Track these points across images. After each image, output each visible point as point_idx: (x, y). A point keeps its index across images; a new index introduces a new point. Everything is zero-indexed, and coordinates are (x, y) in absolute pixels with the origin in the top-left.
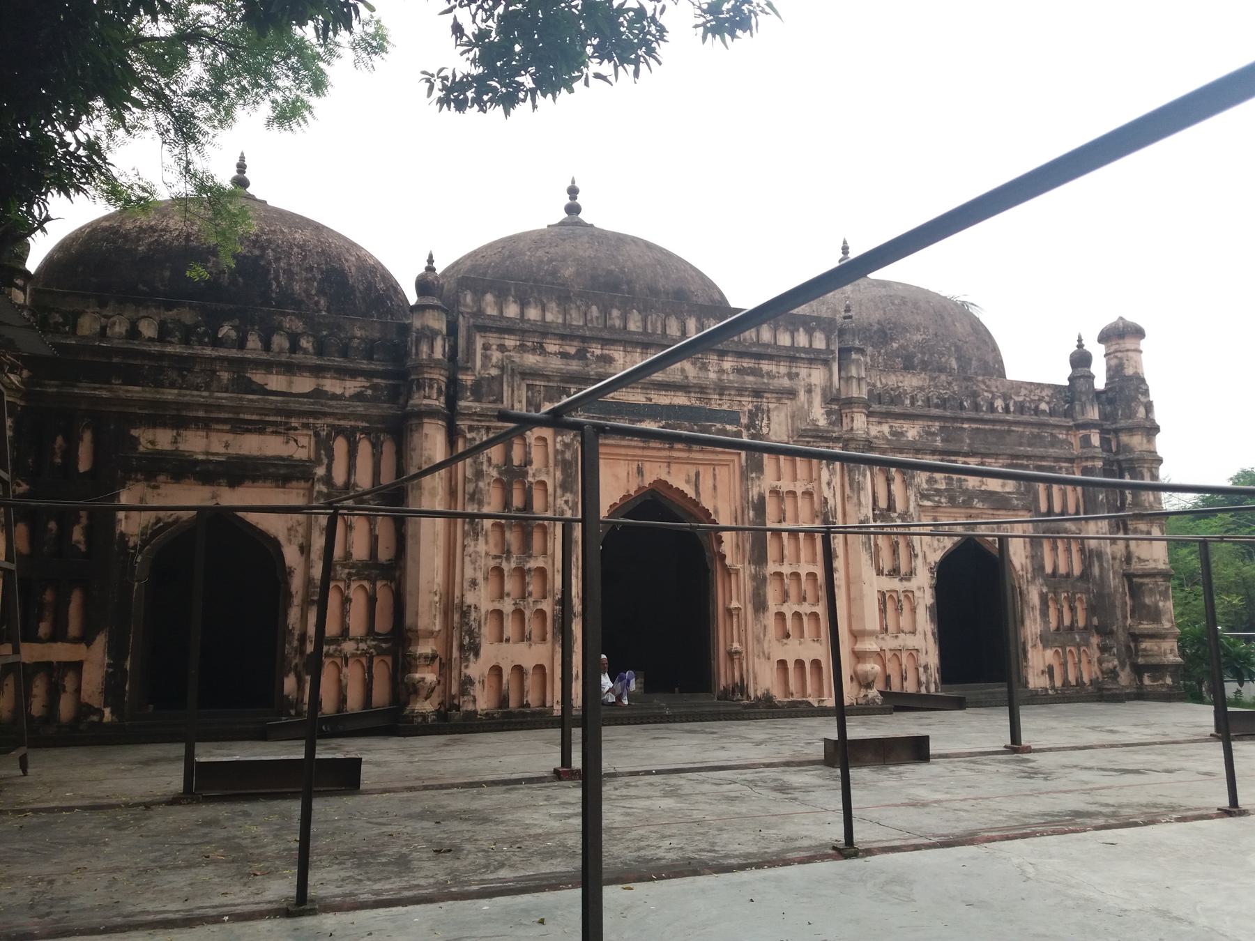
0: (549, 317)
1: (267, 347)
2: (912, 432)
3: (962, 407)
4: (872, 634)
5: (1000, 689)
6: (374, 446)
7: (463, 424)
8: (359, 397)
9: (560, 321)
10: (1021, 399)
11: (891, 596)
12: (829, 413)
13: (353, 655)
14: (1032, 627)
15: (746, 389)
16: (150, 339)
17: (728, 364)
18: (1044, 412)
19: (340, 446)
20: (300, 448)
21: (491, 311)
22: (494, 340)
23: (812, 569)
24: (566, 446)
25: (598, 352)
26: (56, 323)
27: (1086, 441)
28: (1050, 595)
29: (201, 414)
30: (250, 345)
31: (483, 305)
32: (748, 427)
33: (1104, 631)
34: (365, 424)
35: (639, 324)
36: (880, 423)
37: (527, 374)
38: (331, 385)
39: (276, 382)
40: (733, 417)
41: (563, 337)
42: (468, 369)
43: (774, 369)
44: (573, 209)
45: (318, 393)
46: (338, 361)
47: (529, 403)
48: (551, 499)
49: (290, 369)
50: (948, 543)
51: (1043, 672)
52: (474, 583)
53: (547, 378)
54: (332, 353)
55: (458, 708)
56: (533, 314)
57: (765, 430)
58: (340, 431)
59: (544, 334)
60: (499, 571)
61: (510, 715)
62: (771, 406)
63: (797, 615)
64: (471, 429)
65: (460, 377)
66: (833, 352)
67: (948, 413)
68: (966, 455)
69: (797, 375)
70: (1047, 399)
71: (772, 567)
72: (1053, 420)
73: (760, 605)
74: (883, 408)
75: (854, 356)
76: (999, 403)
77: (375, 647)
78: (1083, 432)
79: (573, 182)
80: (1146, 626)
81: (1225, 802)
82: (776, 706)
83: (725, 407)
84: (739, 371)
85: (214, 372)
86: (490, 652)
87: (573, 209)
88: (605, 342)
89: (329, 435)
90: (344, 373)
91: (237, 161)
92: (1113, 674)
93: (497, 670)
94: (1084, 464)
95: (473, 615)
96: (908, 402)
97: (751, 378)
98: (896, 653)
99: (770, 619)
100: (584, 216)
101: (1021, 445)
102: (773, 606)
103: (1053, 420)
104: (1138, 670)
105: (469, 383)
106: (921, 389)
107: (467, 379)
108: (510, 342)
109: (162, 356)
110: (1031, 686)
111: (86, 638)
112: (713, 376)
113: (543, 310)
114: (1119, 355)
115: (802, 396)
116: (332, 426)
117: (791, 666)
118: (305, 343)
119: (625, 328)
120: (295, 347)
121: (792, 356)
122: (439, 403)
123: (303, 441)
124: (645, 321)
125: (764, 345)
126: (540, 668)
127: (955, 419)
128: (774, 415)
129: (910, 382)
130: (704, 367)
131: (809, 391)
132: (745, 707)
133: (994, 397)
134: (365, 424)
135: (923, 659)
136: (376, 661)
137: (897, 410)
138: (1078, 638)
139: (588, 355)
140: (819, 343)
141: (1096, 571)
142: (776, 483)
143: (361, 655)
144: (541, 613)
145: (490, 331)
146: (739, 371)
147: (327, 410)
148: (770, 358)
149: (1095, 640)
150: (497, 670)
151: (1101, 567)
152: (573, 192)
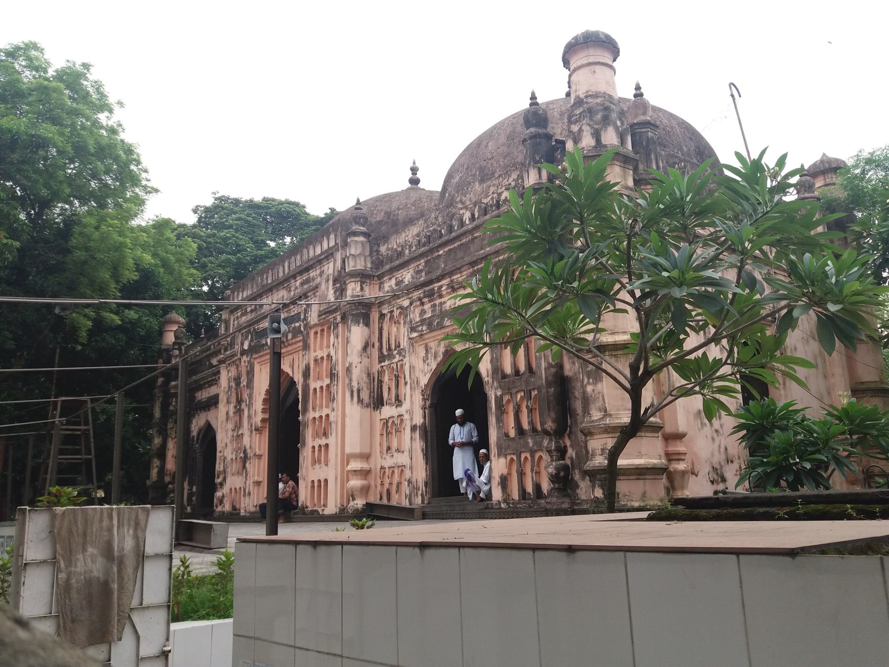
2: (407, 275)
3: (441, 236)
11: (393, 422)
12: (335, 292)
28: (506, 398)
36: (390, 279)
43: (314, 274)
44: (414, 181)
50: (434, 366)
63: (320, 446)
68: (439, 279)
70: (513, 184)
79: (414, 163)
84: (302, 284)
87: (414, 181)
96: (407, 252)
112: (292, 293)
117: (316, 484)
131: (328, 281)
138: (530, 442)
142: (315, 354)
152: (414, 170)
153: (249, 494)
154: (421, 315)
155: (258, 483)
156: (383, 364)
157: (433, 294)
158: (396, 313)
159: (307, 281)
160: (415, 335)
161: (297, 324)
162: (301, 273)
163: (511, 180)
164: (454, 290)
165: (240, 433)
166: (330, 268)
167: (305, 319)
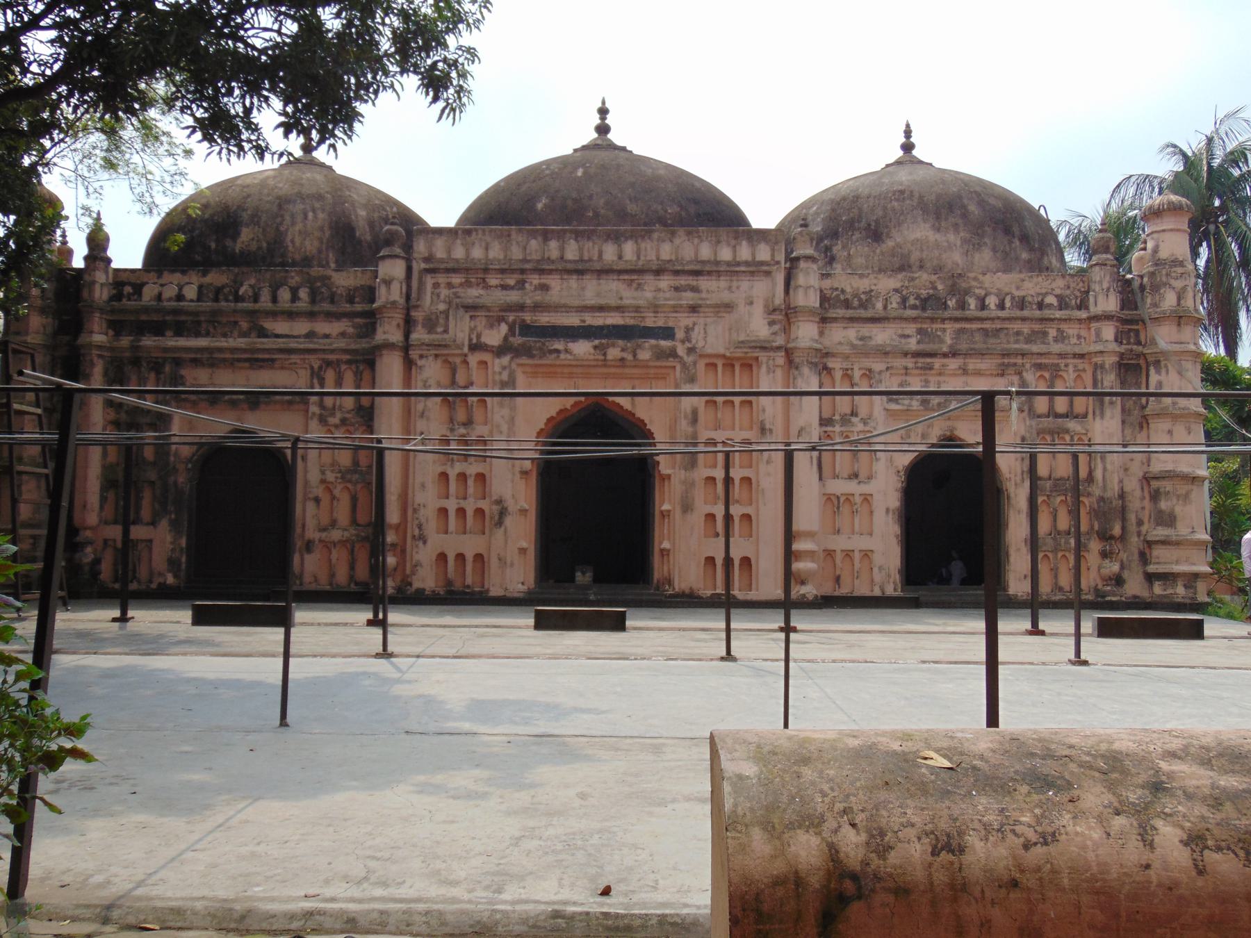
0: (492, 254)
1: (274, 300)
2: (882, 335)
3: (945, 306)
4: (810, 535)
5: (979, 592)
6: (356, 374)
7: (414, 354)
8: (343, 334)
9: (501, 257)
10: (1021, 293)
12: (771, 323)
13: (340, 541)
14: (1017, 529)
15: (681, 306)
16: (192, 301)
17: (665, 282)
18: (1050, 306)
19: (330, 375)
20: (297, 381)
21: (440, 254)
22: (442, 279)
23: (746, 473)
24: (504, 368)
25: (536, 282)
26: (129, 294)
27: (1098, 334)
29: (228, 356)
30: (263, 299)
31: (434, 249)
32: (683, 342)
33: (1105, 536)
34: (348, 357)
35: (577, 253)
37: (471, 308)
38: (322, 327)
39: (281, 327)
40: (668, 333)
41: (503, 271)
42: (417, 307)
45: (311, 335)
46: (326, 306)
47: (472, 330)
48: (489, 415)
49: (291, 315)
51: (1025, 577)
52: (423, 486)
53: (488, 309)
54: (323, 301)
55: (410, 584)
56: (477, 253)
57: (700, 344)
58: (329, 364)
59: (486, 270)
60: (444, 476)
61: (450, 592)
62: (709, 320)
64: (421, 357)
65: (413, 314)
66: (778, 263)
67: (929, 313)
68: (945, 355)
69: (738, 288)
70: (1058, 292)
71: (702, 472)
72: (1058, 314)
73: (687, 508)
74: (850, 313)
75: (802, 264)
76: (992, 301)
77: (357, 535)
78: (1094, 325)
80: (1161, 532)
81: (724, 653)
82: (699, 597)
83: (660, 323)
85: (236, 323)
86: (436, 542)
88: (542, 272)
89: (320, 368)
90: (331, 316)
92: (1118, 581)
93: (442, 557)
94: (1095, 360)
95: (422, 511)
96: (879, 306)
97: (689, 294)
98: (848, 554)
99: (697, 518)
100: (615, 137)
101: (1017, 342)
102: (702, 507)
103: (1058, 314)
104: (1150, 578)
105: (420, 319)
106: (896, 290)
107: (418, 315)
108: (457, 279)
109: (196, 314)
110: (1011, 591)
111: (153, 523)
112: (649, 295)
113: (487, 249)
114: (1155, 236)
115: (742, 309)
116: (323, 360)
118: (303, 294)
119: (562, 258)
120: (295, 298)
121: (733, 270)
122: (396, 336)
123: (302, 372)
124: (581, 249)
125: (703, 262)
126: (479, 558)
127: (933, 320)
128: (711, 330)
129: (887, 284)
130: (640, 287)
132: (671, 596)
133: (986, 295)
134: (348, 357)
135: (878, 559)
136: (357, 546)
137: (862, 313)
139: (527, 285)
140: (763, 253)
141: (1098, 474)
143: (347, 541)
144: (480, 512)
146: (677, 289)
147: (317, 346)
148: (709, 273)
149: (1095, 546)
150: (442, 557)
151: (1105, 469)
153: (512, 565)
154: (901, 385)
155: (523, 551)
156: (829, 429)
157: (931, 369)
158: (857, 374)
159: (695, 289)
160: (893, 406)
161: (663, 343)
162: (677, 273)
163: (1054, 285)
164: (965, 372)
165: (473, 469)
166: (769, 289)
167: (688, 339)
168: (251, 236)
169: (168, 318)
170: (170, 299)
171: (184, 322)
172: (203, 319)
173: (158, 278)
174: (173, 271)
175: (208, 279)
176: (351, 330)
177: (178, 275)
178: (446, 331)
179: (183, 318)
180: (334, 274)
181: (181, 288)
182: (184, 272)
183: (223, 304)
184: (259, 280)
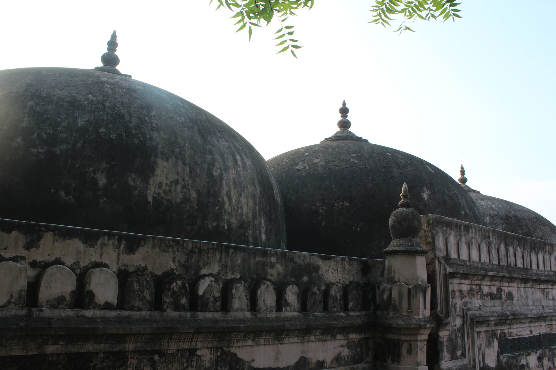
1: (253, 305)
8: (338, 359)
16: (107, 306)
44: (345, 124)
49: (278, 332)
87: (345, 124)
91: (109, 38)
107: (444, 334)
118: (291, 295)
145: (456, 278)
152: (344, 111)
168: (173, 177)
169: (51, 349)
170: (59, 302)
171: (89, 356)
172: (130, 347)
173: (28, 247)
174: (67, 235)
175: (136, 260)
176: (346, 352)
177: (77, 244)
178: (463, 355)
179: (89, 347)
180: (320, 263)
181: (82, 278)
182: (89, 240)
183: (172, 314)
184: (225, 266)
